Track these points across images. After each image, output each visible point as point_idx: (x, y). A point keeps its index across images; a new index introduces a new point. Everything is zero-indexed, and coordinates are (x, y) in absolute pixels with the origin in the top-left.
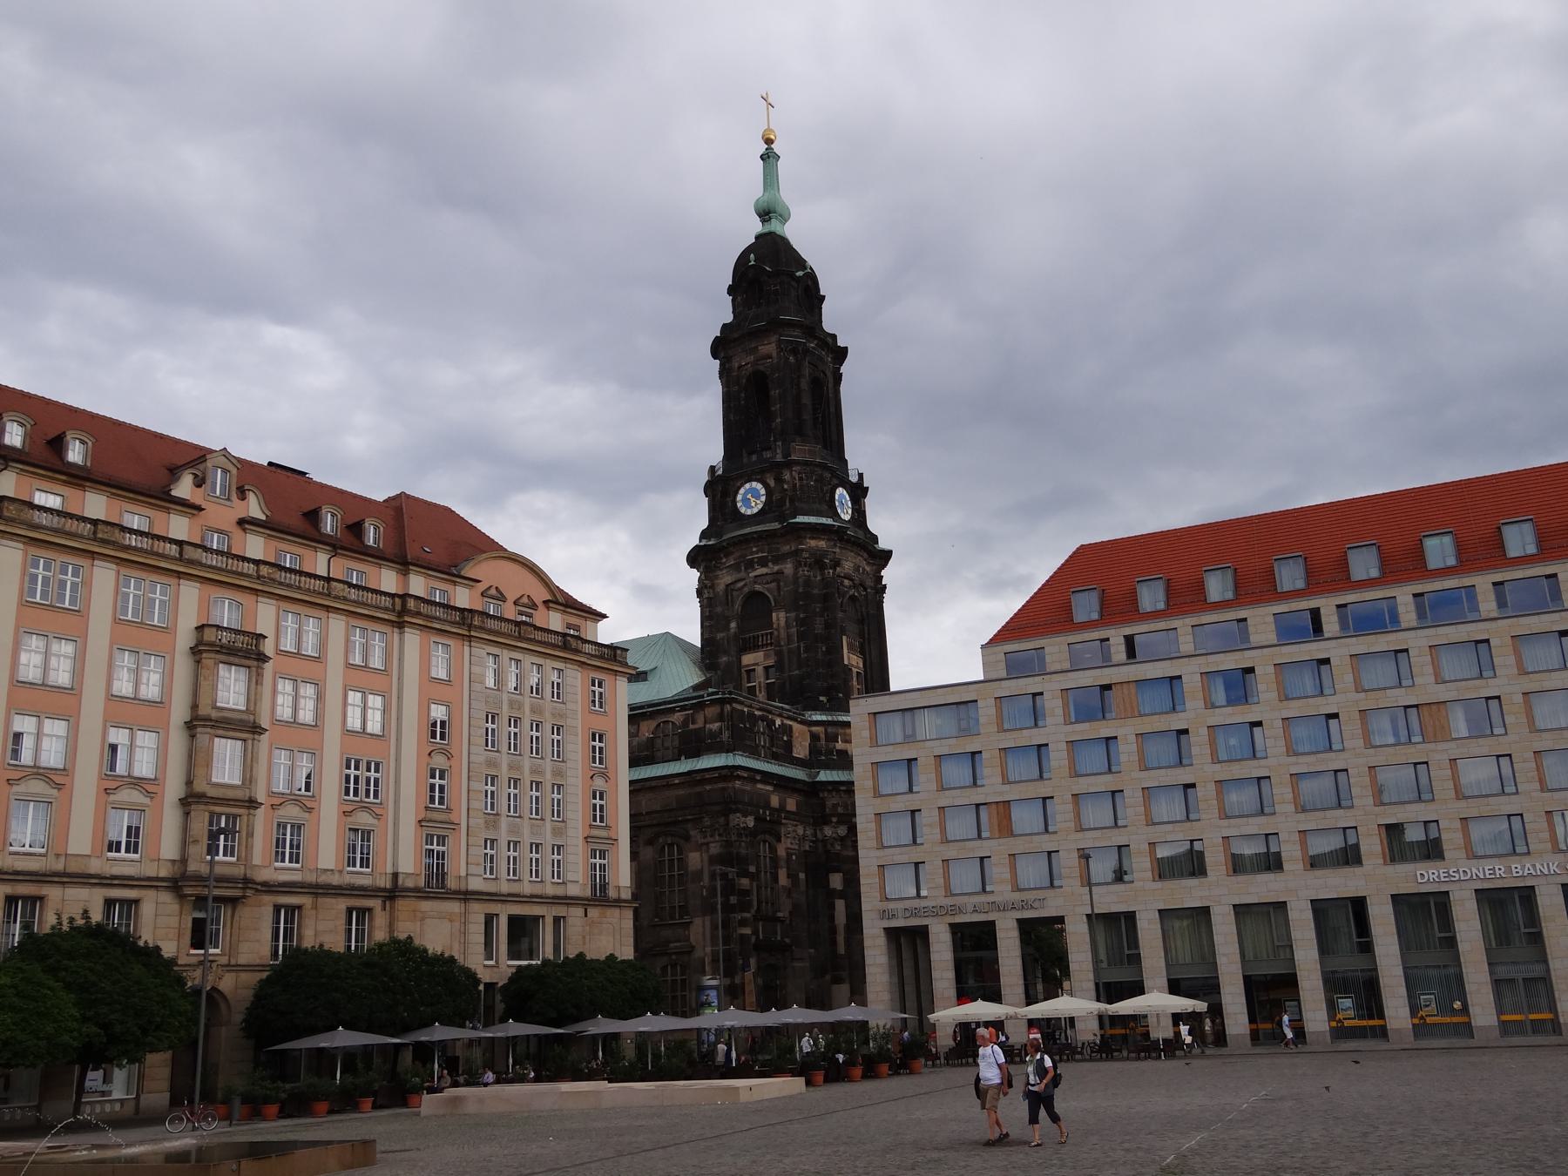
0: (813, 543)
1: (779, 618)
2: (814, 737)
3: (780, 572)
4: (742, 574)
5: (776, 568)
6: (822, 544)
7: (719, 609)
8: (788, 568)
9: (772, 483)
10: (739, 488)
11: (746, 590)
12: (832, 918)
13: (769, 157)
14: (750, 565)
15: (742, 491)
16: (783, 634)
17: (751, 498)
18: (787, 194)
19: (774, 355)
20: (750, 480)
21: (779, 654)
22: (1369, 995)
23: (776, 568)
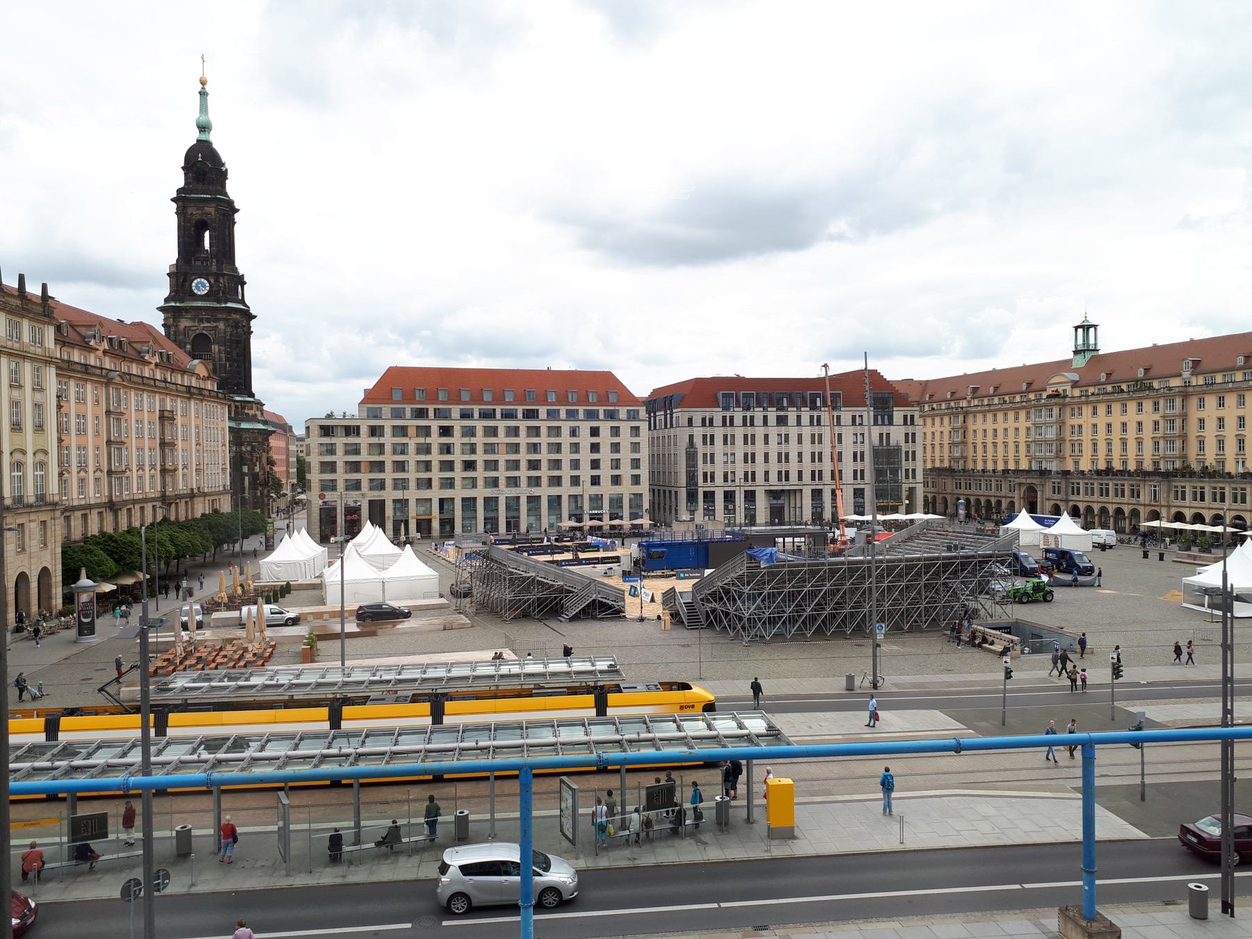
0: (234, 316)
1: (215, 348)
2: (236, 407)
3: (216, 327)
4: (196, 324)
5: (215, 324)
6: (238, 317)
7: (181, 337)
8: (221, 325)
9: (212, 281)
10: (194, 280)
11: (198, 332)
12: (243, 484)
13: (203, 94)
14: (201, 321)
15: (195, 281)
16: (217, 356)
17: (201, 286)
18: (213, 117)
19: (213, 213)
20: (200, 277)
21: (214, 365)
22: (451, 522)
23: (215, 324)
